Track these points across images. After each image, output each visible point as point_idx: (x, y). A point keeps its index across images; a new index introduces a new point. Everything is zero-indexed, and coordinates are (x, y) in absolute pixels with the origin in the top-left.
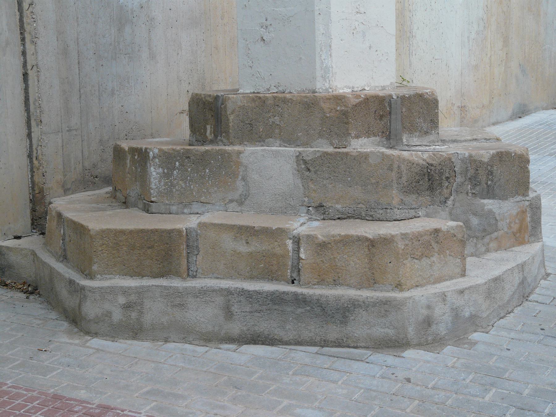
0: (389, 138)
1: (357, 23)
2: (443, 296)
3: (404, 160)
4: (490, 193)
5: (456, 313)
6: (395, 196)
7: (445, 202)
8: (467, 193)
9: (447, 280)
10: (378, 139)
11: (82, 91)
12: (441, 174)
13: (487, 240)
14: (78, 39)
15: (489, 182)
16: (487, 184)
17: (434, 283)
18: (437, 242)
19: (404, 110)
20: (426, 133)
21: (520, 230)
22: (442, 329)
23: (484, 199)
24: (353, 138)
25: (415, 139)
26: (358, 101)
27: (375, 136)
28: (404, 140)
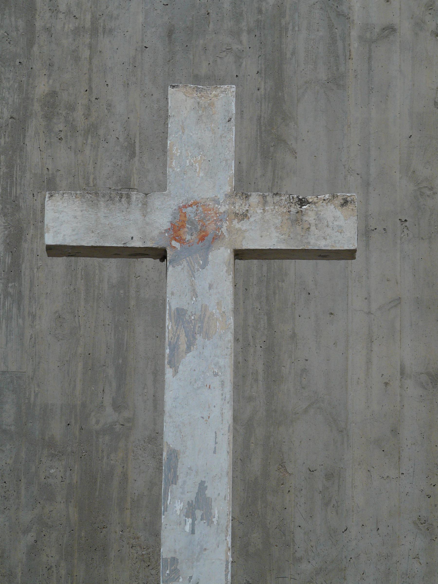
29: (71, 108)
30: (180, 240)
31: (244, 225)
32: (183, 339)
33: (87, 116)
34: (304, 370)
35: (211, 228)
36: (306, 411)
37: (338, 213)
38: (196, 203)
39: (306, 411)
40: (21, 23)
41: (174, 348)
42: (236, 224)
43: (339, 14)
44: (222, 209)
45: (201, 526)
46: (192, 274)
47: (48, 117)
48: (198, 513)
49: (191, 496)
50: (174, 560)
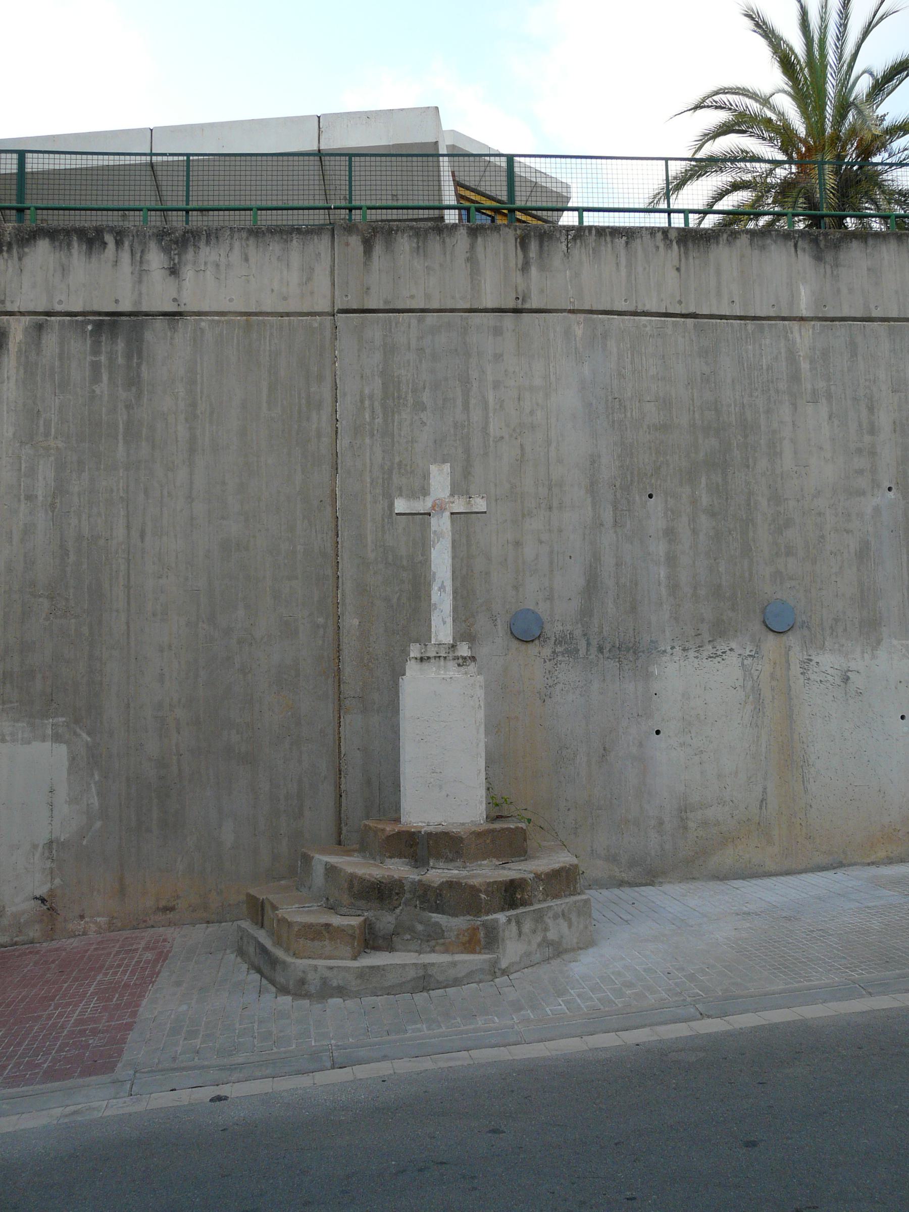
0: (416, 861)
1: (432, 780)
2: (315, 968)
3: (356, 876)
4: (439, 909)
5: (324, 981)
6: (346, 899)
7: (394, 910)
8: (416, 906)
9: (337, 959)
10: (407, 860)
11: (381, 806)
12: (391, 890)
13: (433, 943)
14: (379, 774)
15: (438, 902)
16: (436, 902)
17: (325, 959)
18: (328, 932)
19: (431, 842)
20: (452, 860)
21: (470, 942)
22: (312, 989)
23: (433, 913)
24: (387, 858)
25: (441, 864)
26: (392, 833)
27: (406, 858)
28: (431, 864)
29: (406, 465)
30: (435, 510)
31: (454, 505)
32: (436, 540)
33: (411, 468)
34: (478, 543)
35: (443, 506)
36: (479, 554)
37: (481, 500)
38: (439, 499)
39: (479, 554)
40: (390, 440)
41: (433, 542)
42: (451, 505)
43: (487, 433)
44: (447, 500)
45: (443, 594)
46: (438, 519)
47: (400, 469)
48: (442, 590)
49: (440, 585)
50: (435, 604)
